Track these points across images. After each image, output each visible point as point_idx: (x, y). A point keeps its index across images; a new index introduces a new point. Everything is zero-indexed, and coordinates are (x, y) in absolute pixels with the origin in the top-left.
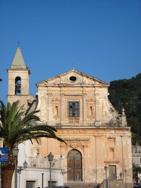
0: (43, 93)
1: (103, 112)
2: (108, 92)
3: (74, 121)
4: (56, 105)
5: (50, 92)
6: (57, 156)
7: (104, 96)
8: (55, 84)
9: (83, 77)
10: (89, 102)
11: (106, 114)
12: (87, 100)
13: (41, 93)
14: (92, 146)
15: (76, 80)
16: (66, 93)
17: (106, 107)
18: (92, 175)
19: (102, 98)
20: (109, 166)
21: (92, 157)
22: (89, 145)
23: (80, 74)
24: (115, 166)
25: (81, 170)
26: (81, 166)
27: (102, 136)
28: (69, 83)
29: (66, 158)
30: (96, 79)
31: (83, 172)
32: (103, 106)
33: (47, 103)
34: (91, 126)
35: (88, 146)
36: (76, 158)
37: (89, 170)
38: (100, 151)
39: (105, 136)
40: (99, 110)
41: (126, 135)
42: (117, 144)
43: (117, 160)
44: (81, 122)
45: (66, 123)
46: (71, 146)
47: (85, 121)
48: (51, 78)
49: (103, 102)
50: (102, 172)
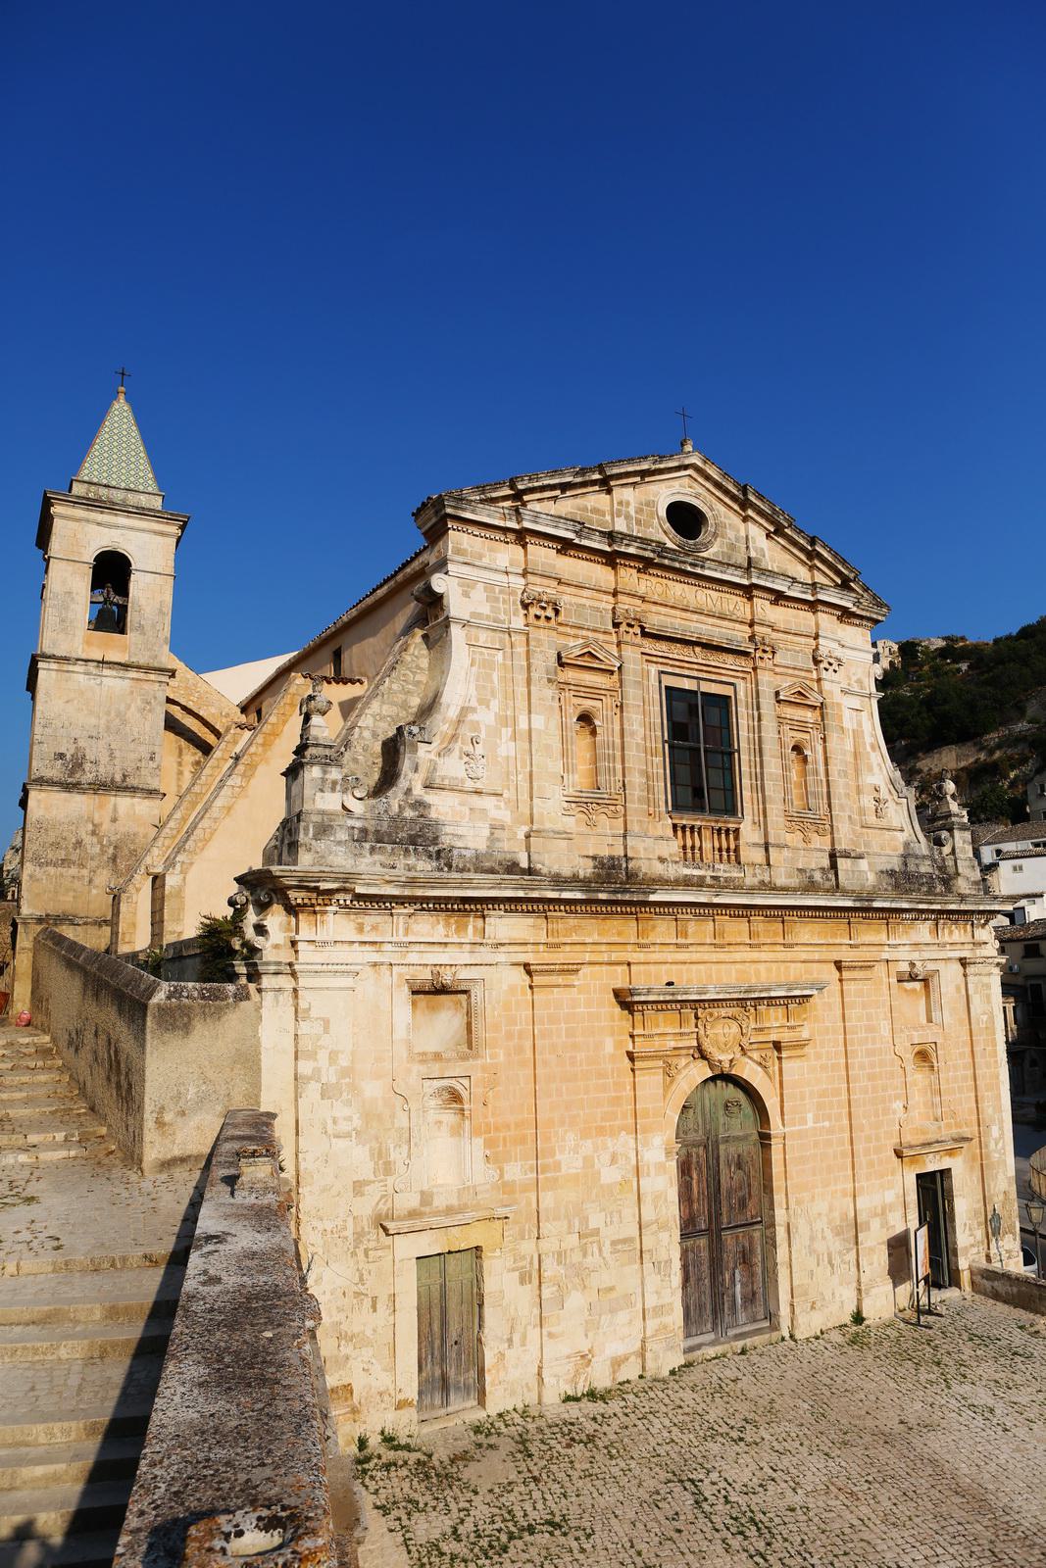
0: (489, 587)
8: (582, 528)
9: (745, 519)
12: (777, 694)
16: (656, 619)
18: (832, 1266)
21: (827, 1124)
23: (734, 498)
28: (670, 545)
30: (825, 554)
33: (521, 677)
44: (752, 855)
48: (555, 473)
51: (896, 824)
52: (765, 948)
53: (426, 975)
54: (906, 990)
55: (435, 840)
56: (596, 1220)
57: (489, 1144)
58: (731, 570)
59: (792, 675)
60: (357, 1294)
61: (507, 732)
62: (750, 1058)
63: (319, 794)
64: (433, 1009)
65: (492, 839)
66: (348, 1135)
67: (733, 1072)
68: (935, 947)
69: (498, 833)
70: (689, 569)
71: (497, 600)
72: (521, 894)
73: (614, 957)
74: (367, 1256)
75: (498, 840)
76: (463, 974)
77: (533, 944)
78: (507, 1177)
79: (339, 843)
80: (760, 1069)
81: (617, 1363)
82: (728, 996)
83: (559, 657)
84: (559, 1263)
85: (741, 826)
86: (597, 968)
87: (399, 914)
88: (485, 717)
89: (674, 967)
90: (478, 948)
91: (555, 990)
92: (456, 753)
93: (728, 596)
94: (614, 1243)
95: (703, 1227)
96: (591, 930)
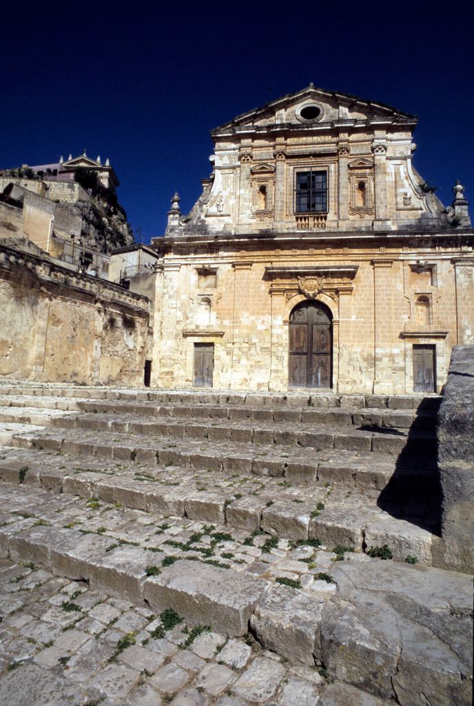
0: (229, 155)
1: (396, 196)
2: (412, 142)
4: (263, 183)
5: (244, 151)
6: (262, 318)
11: (406, 199)
13: (223, 156)
14: (362, 291)
15: (320, 116)
16: (289, 151)
18: (362, 372)
21: (363, 320)
22: (353, 286)
24: (433, 347)
25: (329, 357)
26: (329, 345)
27: (395, 263)
29: (285, 322)
31: (335, 363)
32: (398, 179)
33: (238, 180)
34: (361, 232)
35: (351, 290)
36: (317, 324)
37: (352, 356)
38: (387, 304)
39: (403, 260)
40: (385, 190)
42: (440, 283)
43: (440, 330)
46: (300, 292)
47: (344, 220)
49: (399, 169)
50: (391, 364)
51: (417, 206)
53: (201, 267)
55: (206, 230)
56: (255, 340)
57: (217, 314)
60: (176, 350)
61: (233, 197)
65: (224, 228)
66: (176, 308)
67: (316, 298)
73: (266, 260)
76: (212, 266)
78: (224, 324)
80: (330, 299)
81: (260, 385)
83: (251, 171)
84: (239, 350)
85: (328, 215)
88: (225, 194)
92: (215, 205)
95: (305, 351)
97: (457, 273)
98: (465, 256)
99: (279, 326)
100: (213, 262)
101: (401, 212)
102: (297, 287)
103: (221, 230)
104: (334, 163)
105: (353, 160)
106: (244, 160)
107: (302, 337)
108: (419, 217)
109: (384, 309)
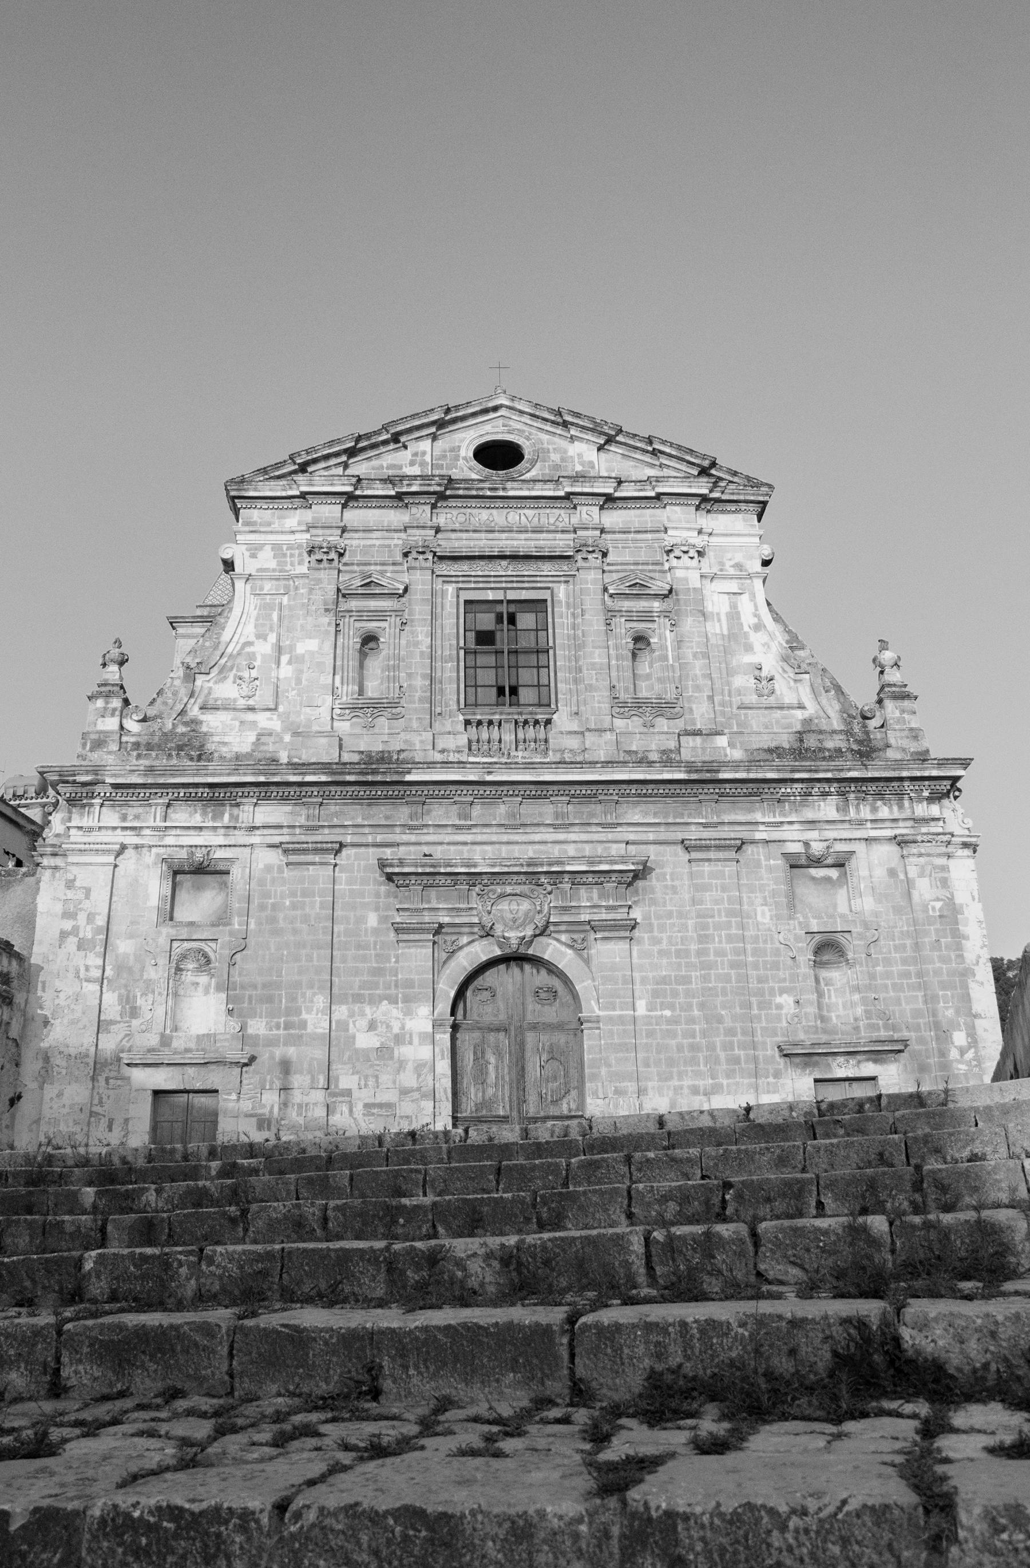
0: (276, 547)
1: (730, 672)
3: (508, 737)
7: (739, 566)
10: (627, 604)
12: (605, 590)
13: (260, 547)
14: (662, 928)
15: (523, 465)
16: (449, 544)
17: (752, 634)
19: (725, 578)
20: (816, 1081)
21: (667, 1013)
22: (636, 914)
28: (474, 476)
29: (437, 1024)
30: (668, 450)
36: (534, 1027)
38: (733, 965)
40: (706, 656)
41: (936, 828)
45: (442, 751)
51: (789, 698)
52: (572, 829)
53: (183, 854)
54: (813, 879)
58: (539, 485)
59: (617, 571)
62: (557, 940)
63: (100, 720)
64: (198, 888)
65: (258, 742)
67: (530, 952)
68: (847, 826)
69: (263, 739)
70: (489, 493)
71: (285, 555)
72: (262, 779)
73: (379, 839)
74: (107, 1083)
75: (264, 744)
76: (219, 854)
77: (289, 827)
78: (250, 1031)
79: (110, 753)
80: (570, 952)
82: (506, 870)
85: (555, 716)
86: (363, 850)
87: (157, 804)
89: (452, 848)
90: (232, 832)
91: (311, 867)
93: (548, 511)
94: (367, 1106)
95: (502, 1113)
96: (355, 814)
97: (910, 876)
98: (924, 830)
99: (423, 1036)
100: (221, 840)
101: (750, 712)
102: (476, 920)
103: (245, 748)
104: (567, 582)
105: (615, 576)
106: (320, 561)
107: (491, 1068)
108: (799, 727)
109: (727, 979)
